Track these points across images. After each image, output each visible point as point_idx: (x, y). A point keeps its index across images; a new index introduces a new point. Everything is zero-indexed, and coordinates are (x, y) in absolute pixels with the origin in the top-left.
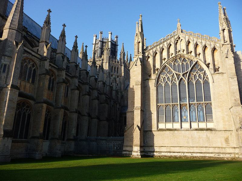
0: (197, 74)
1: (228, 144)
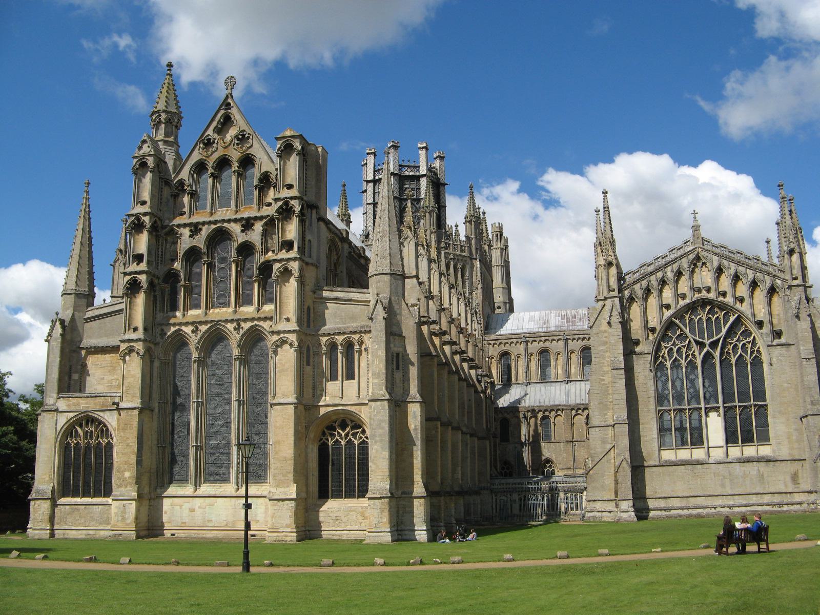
0: (738, 343)
1: (797, 486)
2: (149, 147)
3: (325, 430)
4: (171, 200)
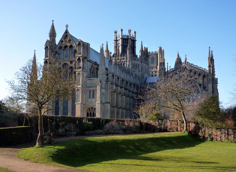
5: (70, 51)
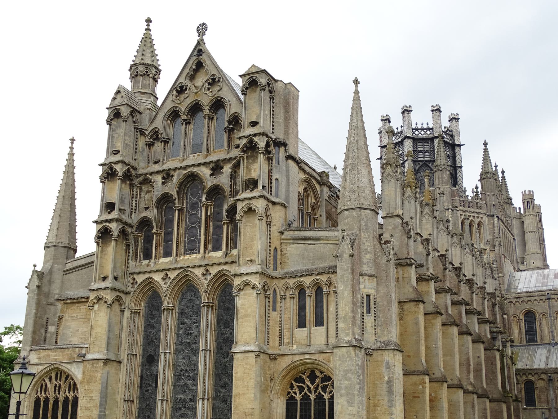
2: (122, 97)
3: (293, 382)
4: (146, 149)
5: (213, 124)
